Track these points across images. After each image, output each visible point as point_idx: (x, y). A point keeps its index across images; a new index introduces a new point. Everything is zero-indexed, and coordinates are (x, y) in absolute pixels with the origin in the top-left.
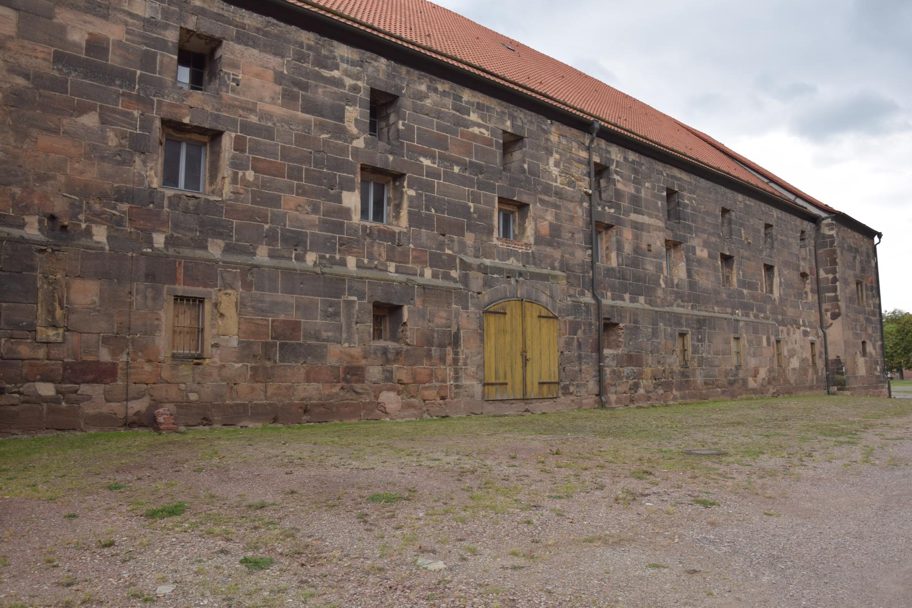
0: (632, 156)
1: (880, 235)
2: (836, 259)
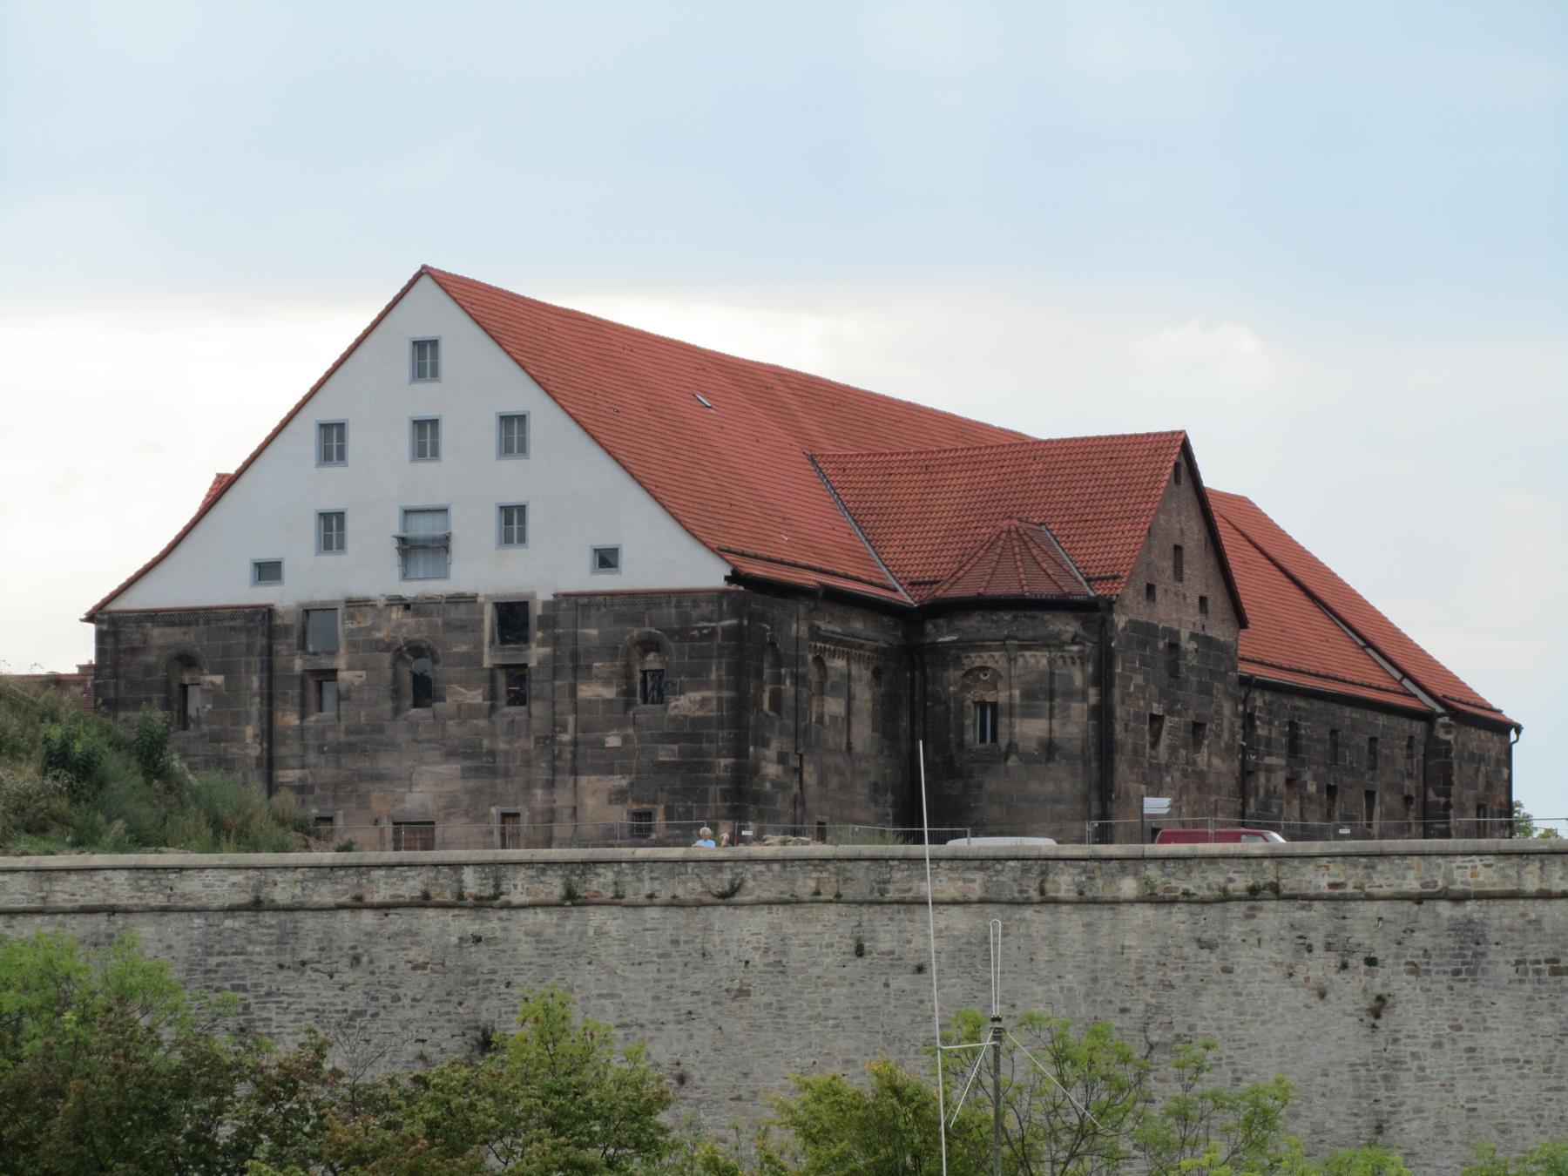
0: (1268, 697)
1: (1518, 729)
2: (1451, 775)
